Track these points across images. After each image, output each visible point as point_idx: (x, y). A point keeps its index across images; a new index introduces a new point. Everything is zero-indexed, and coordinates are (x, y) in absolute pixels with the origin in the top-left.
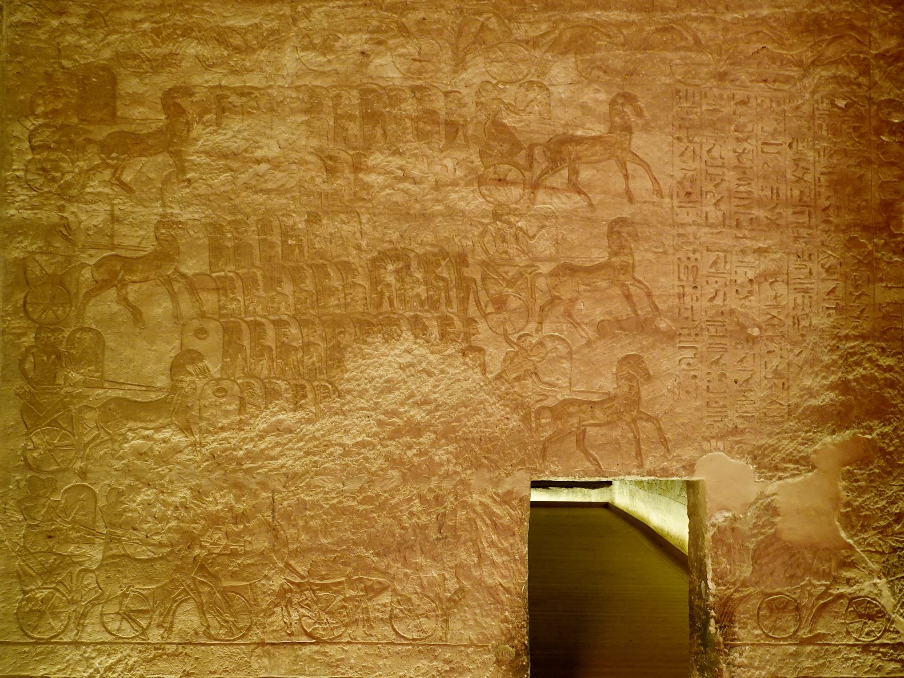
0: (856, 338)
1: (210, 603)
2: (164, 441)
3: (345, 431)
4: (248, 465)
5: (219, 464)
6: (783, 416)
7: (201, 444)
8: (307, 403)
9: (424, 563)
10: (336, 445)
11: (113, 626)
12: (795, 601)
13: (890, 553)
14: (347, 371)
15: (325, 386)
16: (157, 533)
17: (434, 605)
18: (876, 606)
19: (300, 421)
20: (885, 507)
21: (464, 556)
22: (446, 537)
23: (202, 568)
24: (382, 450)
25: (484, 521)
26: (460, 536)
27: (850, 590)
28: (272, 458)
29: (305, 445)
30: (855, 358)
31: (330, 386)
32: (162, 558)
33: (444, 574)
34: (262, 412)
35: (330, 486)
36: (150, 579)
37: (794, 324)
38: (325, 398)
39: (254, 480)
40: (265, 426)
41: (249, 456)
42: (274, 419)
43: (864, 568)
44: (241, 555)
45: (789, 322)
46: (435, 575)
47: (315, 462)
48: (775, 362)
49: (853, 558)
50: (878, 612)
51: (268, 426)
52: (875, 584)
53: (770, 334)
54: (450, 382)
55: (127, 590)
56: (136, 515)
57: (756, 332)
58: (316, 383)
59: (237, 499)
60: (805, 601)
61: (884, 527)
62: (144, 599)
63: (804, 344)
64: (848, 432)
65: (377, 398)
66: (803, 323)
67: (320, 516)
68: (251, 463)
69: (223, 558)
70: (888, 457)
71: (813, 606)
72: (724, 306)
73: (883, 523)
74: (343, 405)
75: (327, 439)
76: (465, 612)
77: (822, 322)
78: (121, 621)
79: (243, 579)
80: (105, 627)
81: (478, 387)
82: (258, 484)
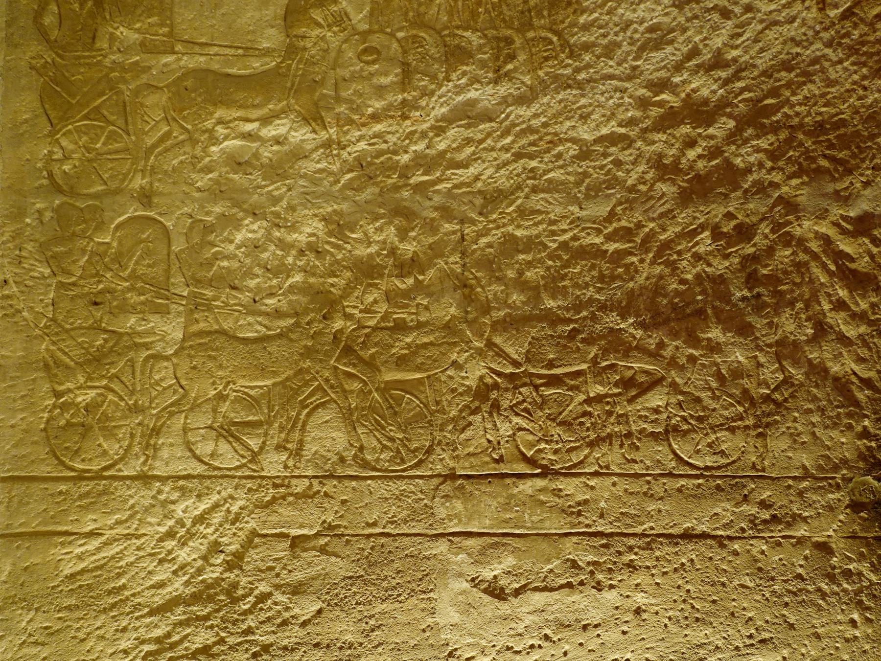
1: (363, 409)
2: (277, 141)
3: (581, 117)
4: (419, 178)
5: (371, 178)
7: (339, 143)
8: (515, 69)
9: (722, 339)
10: (567, 140)
11: (205, 449)
14: (583, 11)
15: (545, 39)
16: (272, 295)
17: (741, 409)
19: (505, 101)
21: (790, 327)
22: (759, 295)
23: (348, 350)
24: (644, 148)
25: (824, 266)
26: (781, 294)
28: (464, 165)
29: (513, 142)
31: (555, 39)
32: (280, 336)
33: (756, 357)
34: (440, 86)
35: (559, 210)
36: (263, 371)
38: (547, 59)
39: (428, 203)
40: (444, 110)
41: (423, 162)
42: (460, 98)
44: (411, 329)
46: (741, 359)
47: (532, 170)
51: (451, 110)
54: (760, 27)
55: (225, 388)
56: (235, 264)
58: (531, 34)
59: (403, 234)
62: (253, 403)
65: (635, 59)
67: (541, 261)
68: (425, 173)
69: (381, 334)
74: (578, 70)
75: (551, 130)
76: (795, 420)
78: (217, 440)
79: (418, 369)
80: (191, 450)
81: (810, 33)
82: (436, 209)
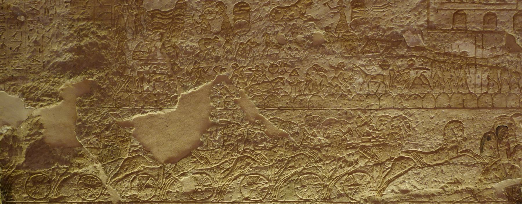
0: (84, 20)
6: (40, 69)
12: (49, 177)
13: (103, 148)
18: (97, 180)
20: (100, 121)
27: (80, 171)
30: (84, 32)
37: (45, 12)
43: (88, 157)
45: (42, 11)
48: (34, 37)
49: (82, 152)
50: (97, 183)
52: (95, 167)
53: (30, 19)
57: (22, 18)
60: (54, 178)
61: (99, 133)
63: (51, 25)
64: (79, 77)
66: (51, 12)
70: (102, 91)
71: (59, 180)
72: (3, 3)
73: (98, 131)
77: (63, 10)
